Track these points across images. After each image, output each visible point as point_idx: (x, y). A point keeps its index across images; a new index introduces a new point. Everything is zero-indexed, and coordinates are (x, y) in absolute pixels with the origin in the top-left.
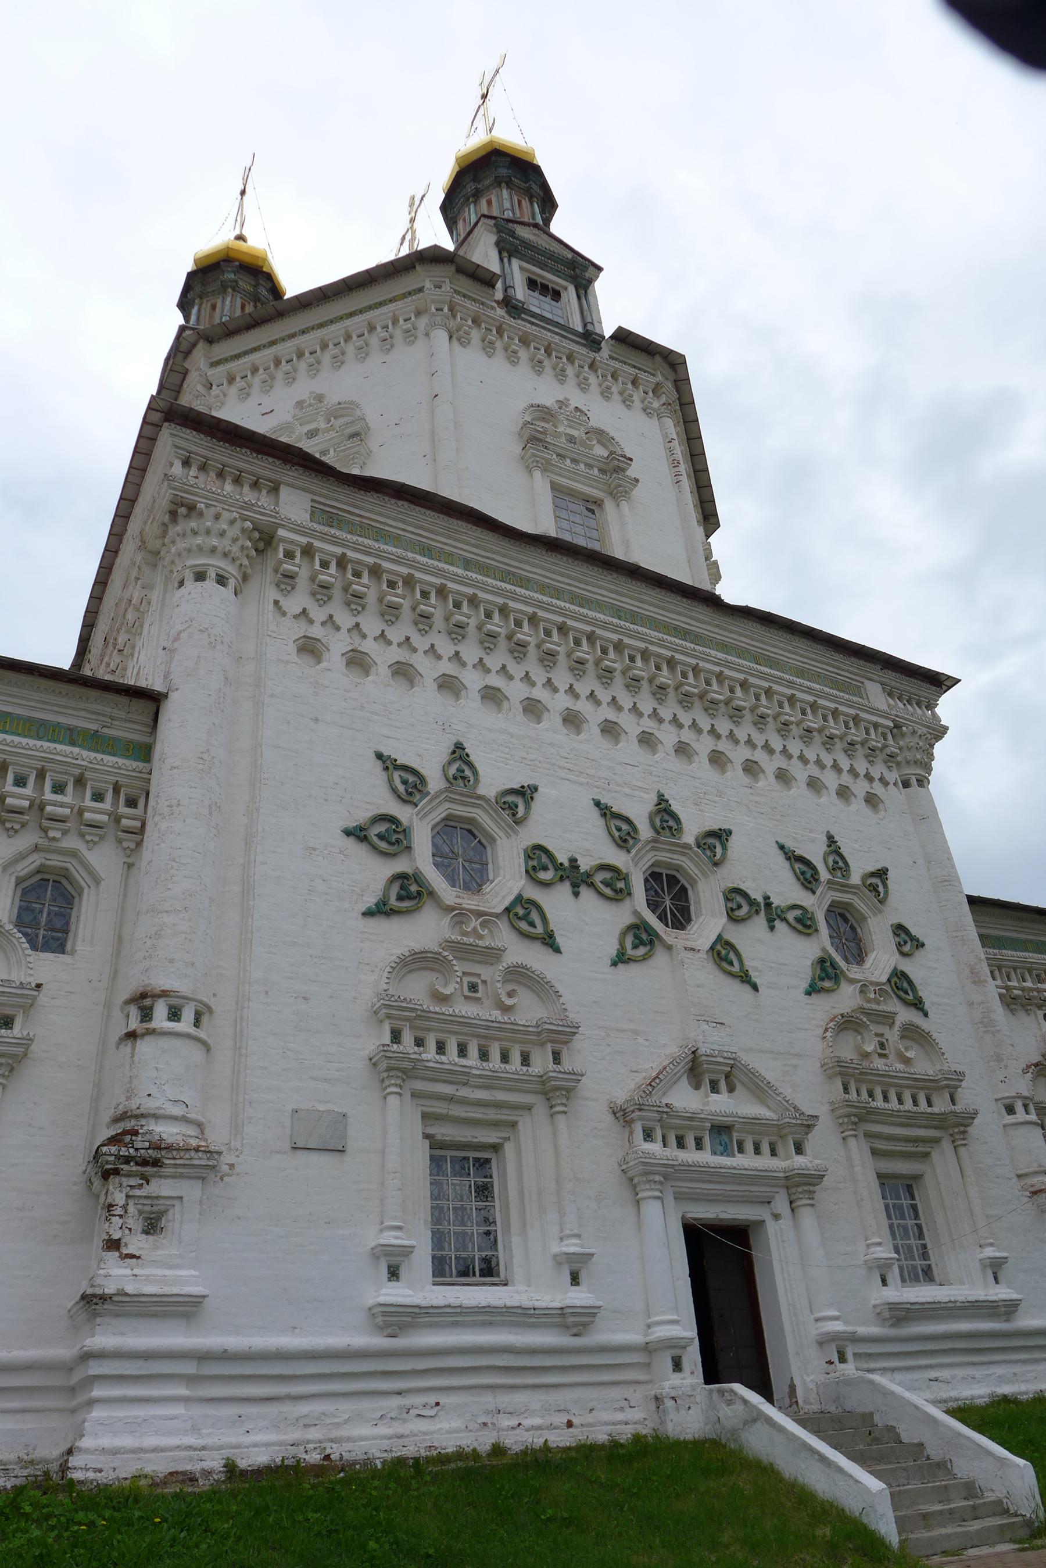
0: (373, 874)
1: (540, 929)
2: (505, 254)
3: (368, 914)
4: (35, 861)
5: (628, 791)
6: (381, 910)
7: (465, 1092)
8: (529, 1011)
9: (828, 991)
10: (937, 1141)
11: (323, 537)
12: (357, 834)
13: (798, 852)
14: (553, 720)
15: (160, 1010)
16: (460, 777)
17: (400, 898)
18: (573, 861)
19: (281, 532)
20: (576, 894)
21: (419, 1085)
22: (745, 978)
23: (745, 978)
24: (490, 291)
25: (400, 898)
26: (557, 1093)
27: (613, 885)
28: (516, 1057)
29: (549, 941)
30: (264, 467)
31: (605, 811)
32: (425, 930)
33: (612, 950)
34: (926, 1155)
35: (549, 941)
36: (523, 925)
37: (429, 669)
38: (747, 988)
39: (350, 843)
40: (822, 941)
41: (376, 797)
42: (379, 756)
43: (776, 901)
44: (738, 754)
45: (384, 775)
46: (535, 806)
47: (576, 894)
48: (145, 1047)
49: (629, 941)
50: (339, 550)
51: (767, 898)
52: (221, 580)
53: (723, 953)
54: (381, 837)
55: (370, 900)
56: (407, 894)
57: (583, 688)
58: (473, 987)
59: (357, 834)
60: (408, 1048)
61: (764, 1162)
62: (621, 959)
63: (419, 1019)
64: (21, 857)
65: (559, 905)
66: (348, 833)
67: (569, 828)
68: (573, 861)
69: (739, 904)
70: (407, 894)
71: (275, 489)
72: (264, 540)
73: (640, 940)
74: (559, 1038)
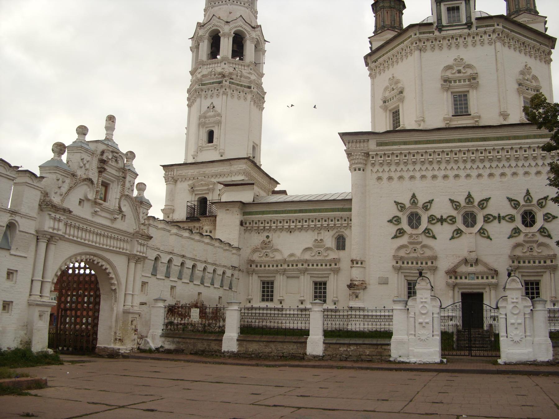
0: (393, 229)
1: (431, 235)
2: (438, 4)
3: (393, 238)
4: (337, 234)
5: (459, 193)
6: (395, 237)
7: (412, 271)
8: (428, 253)
9: (516, 236)
10: (545, 272)
11: (379, 151)
12: (390, 221)
13: (513, 198)
14: (440, 179)
15: (355, 263)
16: (414, 202)
17: (399, 234)
18: (442, 216)
19: (370, 153)
20: (442, 225)
21: (402, 271)
22: (488, 237)
23: (488, 237)
24: (431, 27)
25: (399, 234)
26: (434, 269)
27: (452, 220)
28: (424, 263)
29: (434, 237)
30: (365, 137)
31: (452, 201)
32: (404, 240)
33: (450, 235)
34: (542, 275)
35: (434, 237)
36: (428, 235)
37: (406, 175)
38: (489, 240)
39: (389, 223)
40: (518, 223)
41: (394, 212)
42: (395, 202)
43: (501, 215)
44: (497, 172)
45: (396, 206)
46: (433, 205)
47: (442, 225)
48: (354, 269)
49: (455, 233)
50: (383, 153)
51: (499, 215)
52: (359, 170)
53: (482, 232)
54: (395, 221)
55: (393, 235)
56: (401, 233)
57: (449, 167)
58: (415, 250)
59: (390, 221)
60: (400, 263)
61: (485, 281)
62: (453, 238)
63: (401, 258)
64: (335, 234)
65: (437, 229)
66: (388, 221)
67: (441, 208)
68: (442, 216)
69: (487, 219)
70: (401, 233)
71: (368, 140)
72: (367, 155)
73: (458, 232)
74: (434, 259)
